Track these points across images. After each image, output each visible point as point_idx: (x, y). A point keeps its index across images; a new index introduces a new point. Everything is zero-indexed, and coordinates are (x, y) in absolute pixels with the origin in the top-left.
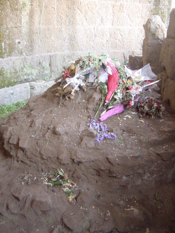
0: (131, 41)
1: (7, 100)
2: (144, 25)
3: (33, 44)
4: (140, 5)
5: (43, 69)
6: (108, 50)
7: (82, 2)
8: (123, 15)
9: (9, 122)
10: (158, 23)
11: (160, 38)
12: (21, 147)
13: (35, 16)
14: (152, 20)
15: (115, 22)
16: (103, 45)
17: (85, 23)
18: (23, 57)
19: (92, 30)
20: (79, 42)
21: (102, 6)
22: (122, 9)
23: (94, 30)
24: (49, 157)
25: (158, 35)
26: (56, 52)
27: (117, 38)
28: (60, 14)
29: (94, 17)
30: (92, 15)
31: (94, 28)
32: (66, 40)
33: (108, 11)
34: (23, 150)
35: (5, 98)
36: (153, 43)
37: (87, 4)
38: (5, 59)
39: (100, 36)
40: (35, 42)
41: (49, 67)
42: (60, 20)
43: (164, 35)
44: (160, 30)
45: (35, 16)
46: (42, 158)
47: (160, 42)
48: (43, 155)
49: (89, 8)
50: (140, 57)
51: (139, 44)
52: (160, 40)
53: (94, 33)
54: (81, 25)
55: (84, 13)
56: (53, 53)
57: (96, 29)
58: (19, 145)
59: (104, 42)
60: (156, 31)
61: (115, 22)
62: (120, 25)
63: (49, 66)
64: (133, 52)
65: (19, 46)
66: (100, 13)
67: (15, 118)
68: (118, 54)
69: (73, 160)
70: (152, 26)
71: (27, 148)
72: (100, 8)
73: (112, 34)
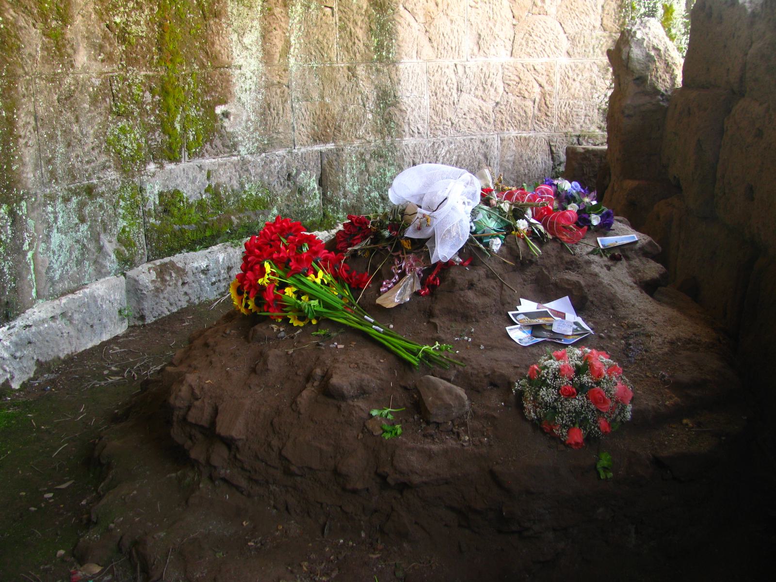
0: (571, 102)
1: (190, 291)
2: (609, 53)
5: (300, 193)
6: (499, 131)
8: (543, 24)
10: (655, 42)
11: (662, 90)
12: (222, 434)
13: (275, 32)
14: (635, 32)
15: (521, 44)
16: (485, 119)
17: (427, 51)
19: (450, 73)
20: (409, 109)
23: (456, 73)
24: (310, 469)
25: (654, 79)
27: (526, 95)
28: (351, 25)
29: (455, 31)
30: (449, 23)
33: (498, 14)
34: (229, 443)
38: (183, 165)
39: (473, 89)
40: (274, 113)
41: (318, 189)
42: (350, 44)
43: (673, 78)
44: (660, 65)
45: (275, 32)
46: (288, 472)
47: (663, 101)
48: (288, 461)
49: (437, 5)
50: (602, 151)
51: (596, 111)
52: (663, 95)
53: (454, 81)
57: (460, 69)
58: (217, 429)
59: (488, 107)
60: (647, 68)
61: (521, 44)
62: (535, 55)
63: (316, 187)
64: (579, 136)
65: (225, 125)
66: (472, 19)
67: (206, 345)
68: (531, 144)
69: (383, 478)
70: (636, 53)
71: (240, 439)
73: (510, 83)
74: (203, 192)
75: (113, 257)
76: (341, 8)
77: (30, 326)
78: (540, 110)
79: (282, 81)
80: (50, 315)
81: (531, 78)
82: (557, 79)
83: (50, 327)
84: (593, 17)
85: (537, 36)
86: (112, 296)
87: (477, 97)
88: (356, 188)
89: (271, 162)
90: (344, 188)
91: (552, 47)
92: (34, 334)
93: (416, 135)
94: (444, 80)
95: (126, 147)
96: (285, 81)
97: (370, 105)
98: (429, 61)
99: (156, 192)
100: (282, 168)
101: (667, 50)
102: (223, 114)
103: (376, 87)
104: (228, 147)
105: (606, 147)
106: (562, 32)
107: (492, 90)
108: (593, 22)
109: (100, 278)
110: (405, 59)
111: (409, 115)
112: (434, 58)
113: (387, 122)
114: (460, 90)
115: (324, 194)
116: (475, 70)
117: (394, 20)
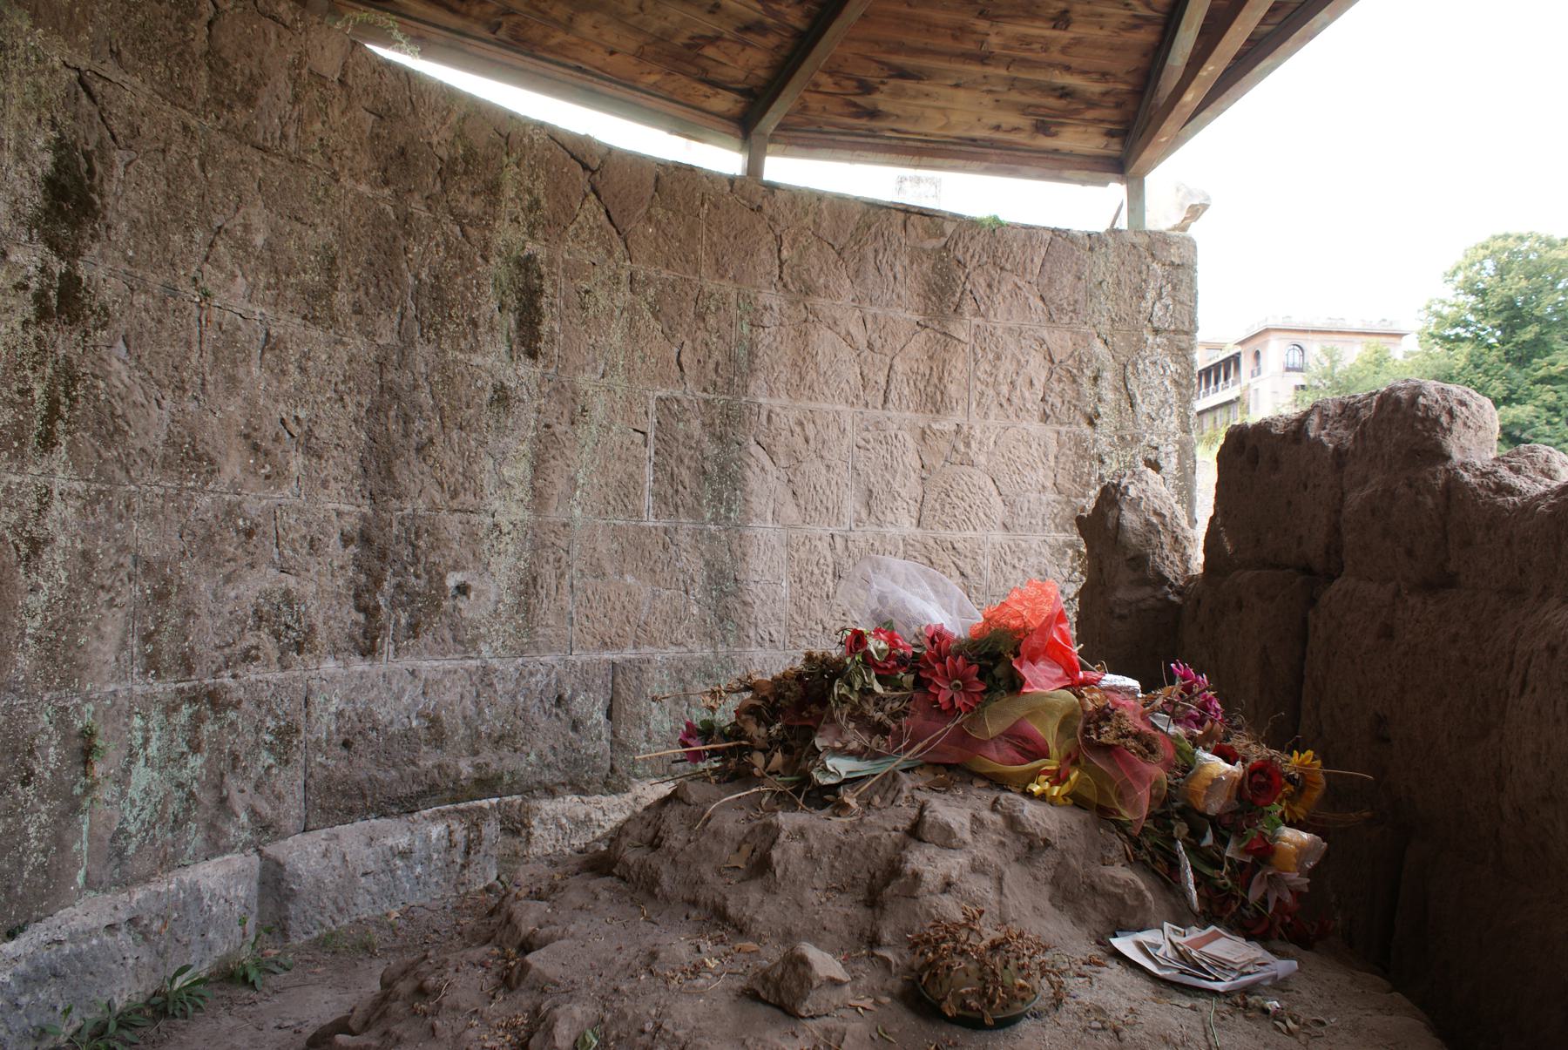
1: (375, 889)
3: (533, 601)
4: (1049, 432)
7: (778, 410)
9: (384, 1015)
10: (1157, 504)
14: (1126, 488)
17: (790, 511)
18: (478, 662)
19: (823, 547)
21: (869, 436)
22: (962, 448)
23: (832, 548)
26: (646, 650)
30: (824, 471)
32: (697, 591)
35: (365, 874)
36: (1138, 601)
37: (801, 424)
38: (382, 666)
40: (543, 593)
43: (1185, 560)
44: (1166, 539)
49: (807, 441)
52: (1171, 586)
53: (830, 560)
55: (783, 463)
56: (629, 653)
60: (1148, 541)
61: (933, 509)
65: (461, 605)
66: (860, 466)
67: (421, 992)
70: (1130, 519)
72: (862, 443)
74: (413, 715)
75: (244, 818)
79: (558, 542)
82: (986, 563)
84: (1041, 472)
86: (232, 891)
88: (667, 726)
90: (648, 724)
93: (767, 644)
94: (814, 558)
95: (288, 627)
96: (563, 543)
97: (697, 591)
98: (793, 527)
100: (548, 685)
101: (1174, 516)
102: (458, 588)
103: (707, 563)
104: (462, 643)
106: (995, 493)
108: (1041, 479)
109: (214, 856)
110: (755, 522)
111: (758, 612)
112: (799, 522)
113: (722, 621)
114: (837, 576)
115: (614, 733)
116: (863, 544)
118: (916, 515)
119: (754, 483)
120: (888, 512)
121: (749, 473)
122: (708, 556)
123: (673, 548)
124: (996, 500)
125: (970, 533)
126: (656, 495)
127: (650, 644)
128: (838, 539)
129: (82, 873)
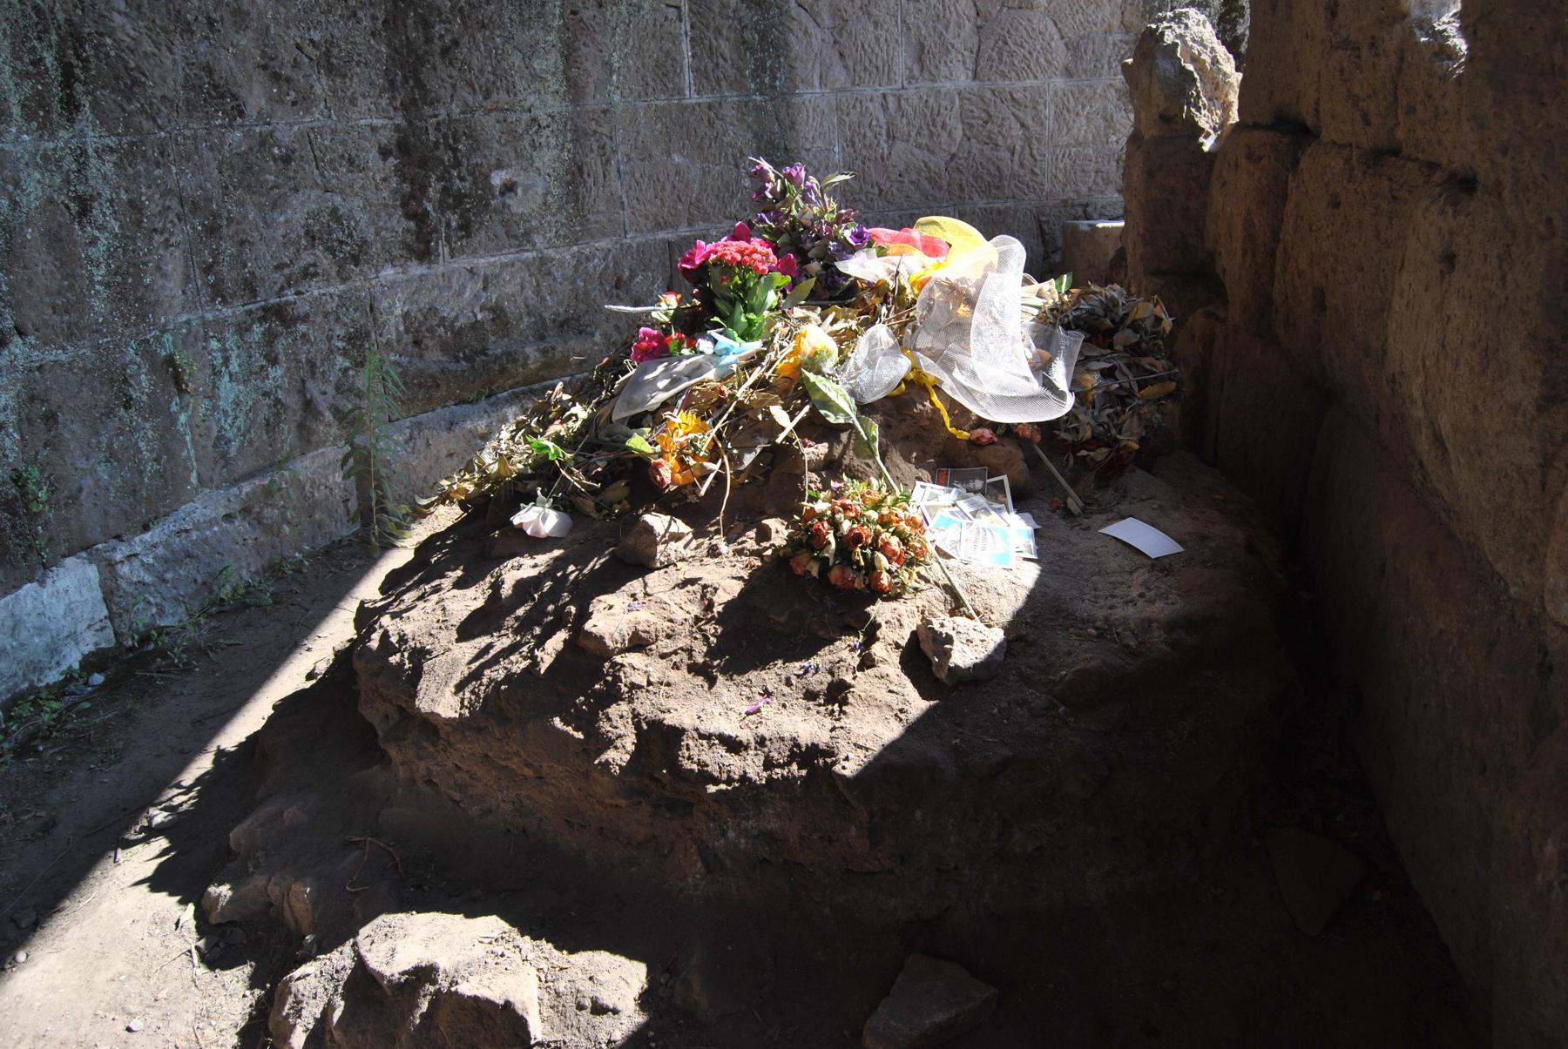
14: (1162, 34)
15: (990, 58)
16: (933, 181)
17: (839, 75)
19: (874, 108)
23: (885, 108)
27: (1000, 141)
30: (871, 29)
31: (884, 96)
40: (590, 181)
42: (711, 66)
45: (584, 50)
51: (1114, 163)
54: (817, 83)
57: (892, 105)
61: (990, 58)
64: (1087, 205)
65: (509, 201)
66: (910, 20)
74: (477, 310)
75: (328, 416)
76: (695, 8)
77: (187, 531)
78: (1022, 165)
80: (222, 512)
81: (1008, 113)
82: (1049, 112)
83: (225, 532)
85: (1015, 43)
87: (919, 146)
89: (588, 259)
91: (1042, 60)
92: (194, 543)
94: (866, 122)
95: (341, 243)
96: (605, 130)
98: (842, 90)
99: (398, 312)
100: (606, 267)
102: (505, 185)
103: (755, 135)
104: (515, 237)
105: (1121, 224)
106: (1057, 36)
107: (945, 135)
114: (891, 137)
117: (782, 24)
118: (972, 67)
119: (797, 48)
120: (942, 67)
121: (792, 38)
122: (755, 128)
123: (718, 124)
124: (1057, 44)
125: (1028, 82)
126: (695, 70)
127: (705, 221)
128: (890, 99)
129: (194, 474)
